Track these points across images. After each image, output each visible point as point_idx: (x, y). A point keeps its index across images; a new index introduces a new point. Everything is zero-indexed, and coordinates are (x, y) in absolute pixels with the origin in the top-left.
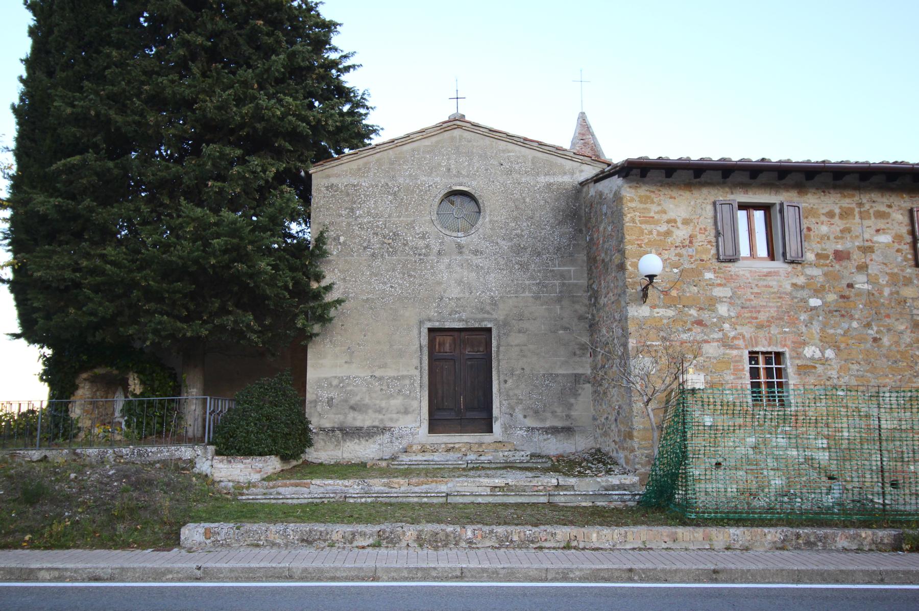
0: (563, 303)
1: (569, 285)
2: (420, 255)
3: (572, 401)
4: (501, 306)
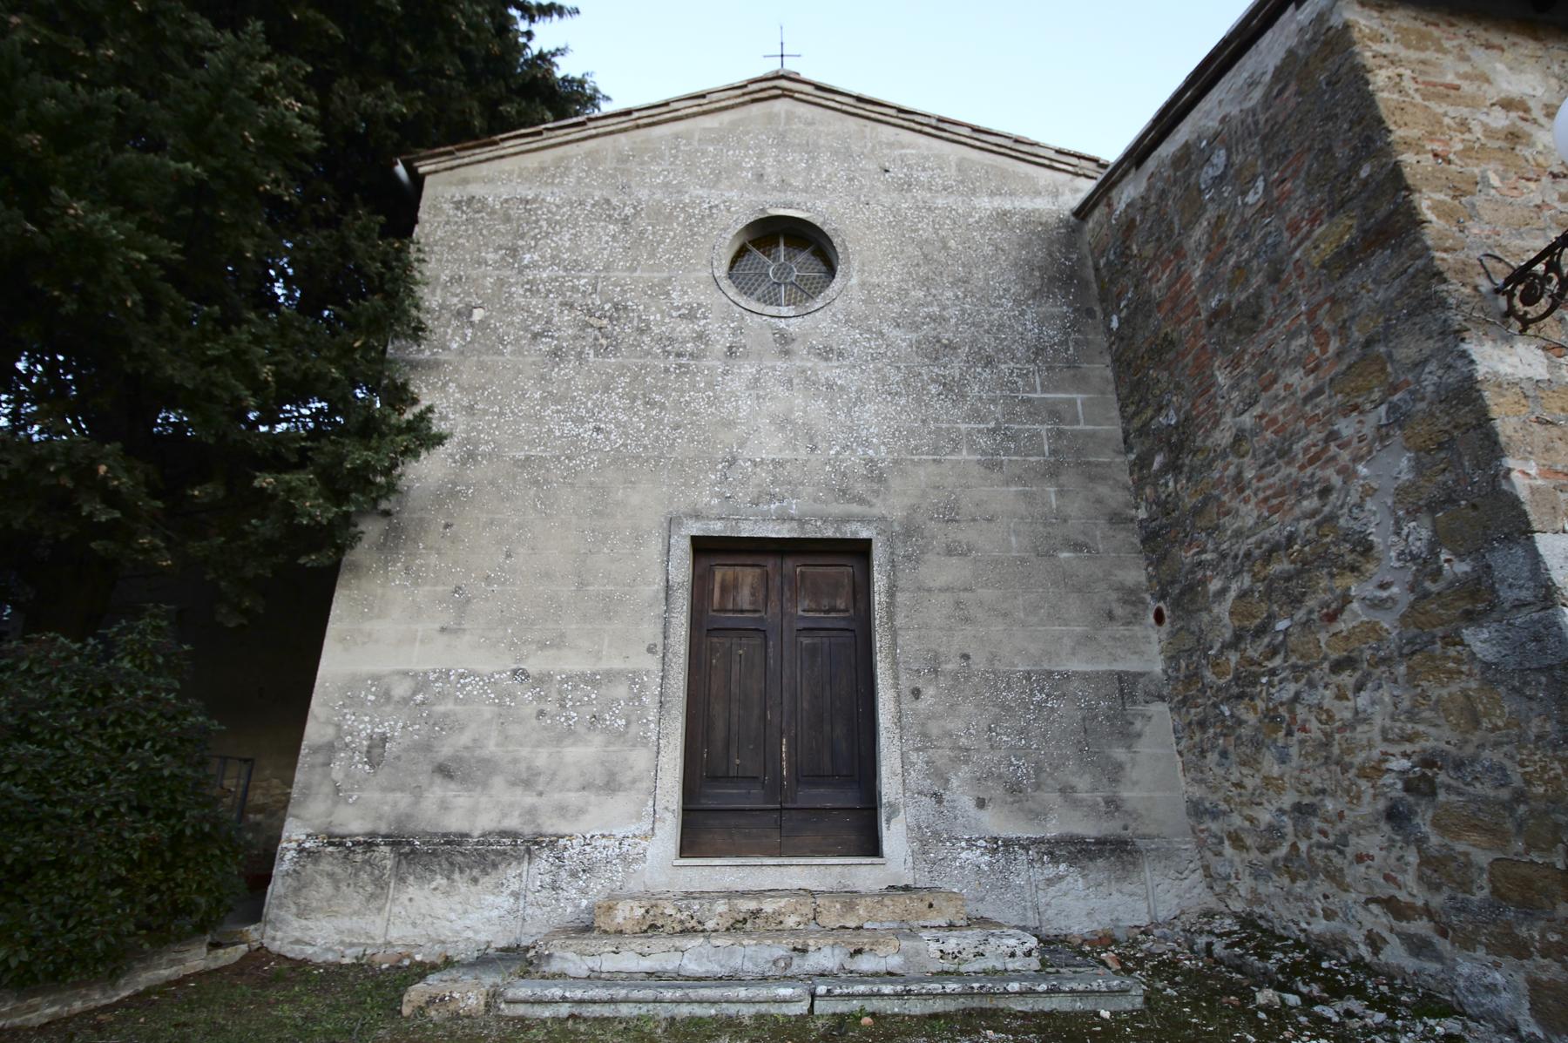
0: (1063, 479)
1: (1075, 435)
2: (679, 355)
3: (1119, 753)
4: (895, 483)
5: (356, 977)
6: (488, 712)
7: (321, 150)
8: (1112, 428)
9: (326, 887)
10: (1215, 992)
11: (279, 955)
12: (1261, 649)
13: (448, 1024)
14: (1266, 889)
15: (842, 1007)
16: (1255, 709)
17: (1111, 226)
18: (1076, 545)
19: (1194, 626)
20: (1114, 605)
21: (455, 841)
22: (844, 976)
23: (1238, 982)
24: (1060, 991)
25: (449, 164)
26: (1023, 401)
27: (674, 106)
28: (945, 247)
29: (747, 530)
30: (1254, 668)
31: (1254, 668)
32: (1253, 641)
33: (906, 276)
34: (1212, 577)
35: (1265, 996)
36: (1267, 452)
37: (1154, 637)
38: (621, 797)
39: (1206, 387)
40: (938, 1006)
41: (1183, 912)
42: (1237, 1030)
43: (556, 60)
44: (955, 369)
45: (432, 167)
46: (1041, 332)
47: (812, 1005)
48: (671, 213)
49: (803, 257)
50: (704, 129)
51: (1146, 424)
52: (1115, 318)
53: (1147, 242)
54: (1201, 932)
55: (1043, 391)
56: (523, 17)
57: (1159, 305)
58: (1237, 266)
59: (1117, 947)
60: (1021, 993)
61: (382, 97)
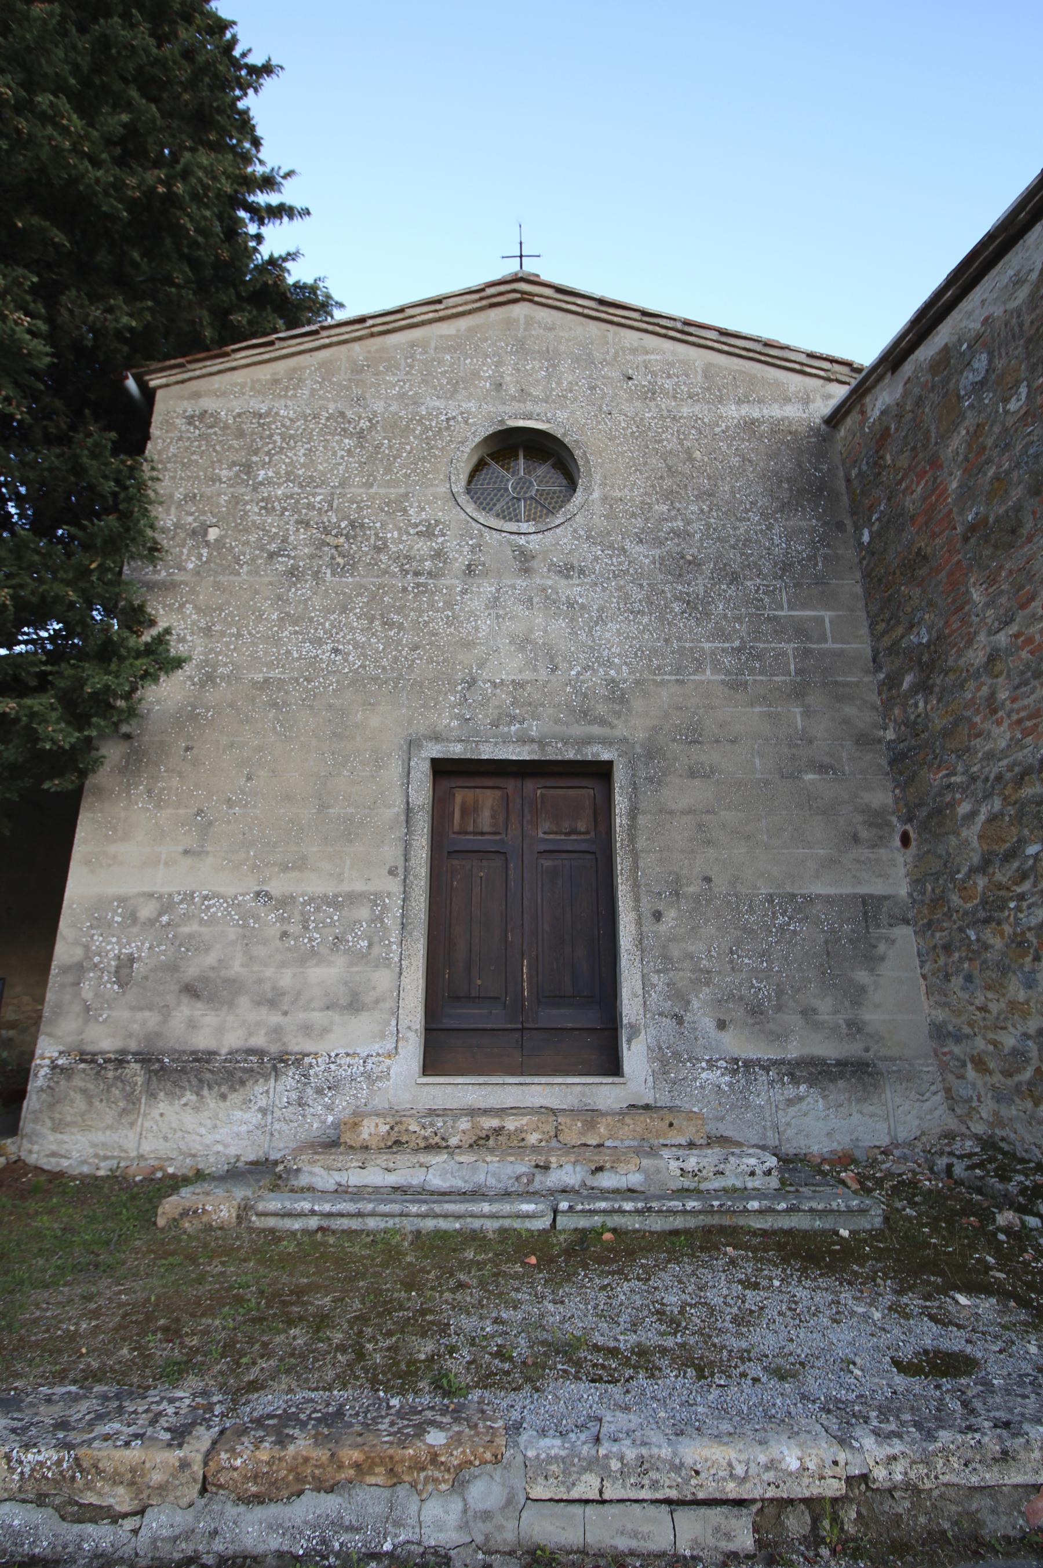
0: (810, 699)
1: (823, 653)
2: (417, 574)
3: (862, 976)
4: (638, 704)
5: (112, 1190)
6: (232, 933)
7: (52, 365)
8: (861, 646)
9: (80, 1103)
10: (954, 1213)
11: (36, 1168)
12: (1010, 874)
13: (202, 1236)
14: (1009, 1112)
15: (583, 1223)
16: (1002, 934)
17: (863, 434)
18: (821, 766)
19: (941, 850)
20: (859, 827)
21: (203, 1058)
22: (585, 1192)
23: (979, 1203)
24: (799, 1210)
25: (180, 377)
26: (769, 618)
27: (410, 312)
28: (690, 459)
29: (487, 752)
30: (1003, 893)
31: (1003, 893)
32: (1002, 866)
33: (650, 490)
34: (961, 800)
35: (1006, 1217)
36: (1023, 673)
37: (900, 860)
38: (364, 1017)
39: (960, 604)
40: (678, 1223)
41: (923, 1134)
42: (977, 1251)
43: (288, 265)
44: (699, 586)
45: (164, 381)
46: (789, 546)
47: (554, 1220)
48: (407, 426)
49: (543, 469)
50: (441, 336)
51: (896, 643)
52: (866, 532)
53: (902, 452)
54: (941, 1153)
55: (790, 608)
56: (252, 220)
57: (913, 518)
58: (997, 478)
59: (857, 1166)
60: (760, 1212)
61: (110, 310)
